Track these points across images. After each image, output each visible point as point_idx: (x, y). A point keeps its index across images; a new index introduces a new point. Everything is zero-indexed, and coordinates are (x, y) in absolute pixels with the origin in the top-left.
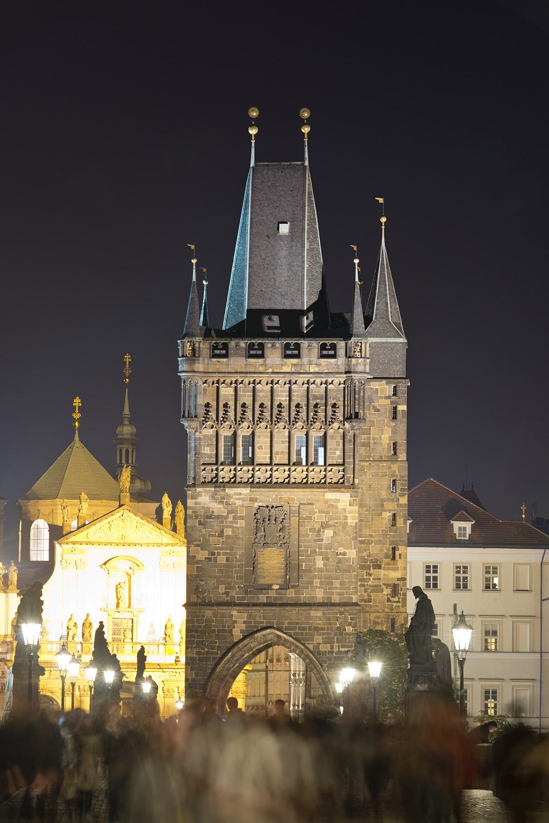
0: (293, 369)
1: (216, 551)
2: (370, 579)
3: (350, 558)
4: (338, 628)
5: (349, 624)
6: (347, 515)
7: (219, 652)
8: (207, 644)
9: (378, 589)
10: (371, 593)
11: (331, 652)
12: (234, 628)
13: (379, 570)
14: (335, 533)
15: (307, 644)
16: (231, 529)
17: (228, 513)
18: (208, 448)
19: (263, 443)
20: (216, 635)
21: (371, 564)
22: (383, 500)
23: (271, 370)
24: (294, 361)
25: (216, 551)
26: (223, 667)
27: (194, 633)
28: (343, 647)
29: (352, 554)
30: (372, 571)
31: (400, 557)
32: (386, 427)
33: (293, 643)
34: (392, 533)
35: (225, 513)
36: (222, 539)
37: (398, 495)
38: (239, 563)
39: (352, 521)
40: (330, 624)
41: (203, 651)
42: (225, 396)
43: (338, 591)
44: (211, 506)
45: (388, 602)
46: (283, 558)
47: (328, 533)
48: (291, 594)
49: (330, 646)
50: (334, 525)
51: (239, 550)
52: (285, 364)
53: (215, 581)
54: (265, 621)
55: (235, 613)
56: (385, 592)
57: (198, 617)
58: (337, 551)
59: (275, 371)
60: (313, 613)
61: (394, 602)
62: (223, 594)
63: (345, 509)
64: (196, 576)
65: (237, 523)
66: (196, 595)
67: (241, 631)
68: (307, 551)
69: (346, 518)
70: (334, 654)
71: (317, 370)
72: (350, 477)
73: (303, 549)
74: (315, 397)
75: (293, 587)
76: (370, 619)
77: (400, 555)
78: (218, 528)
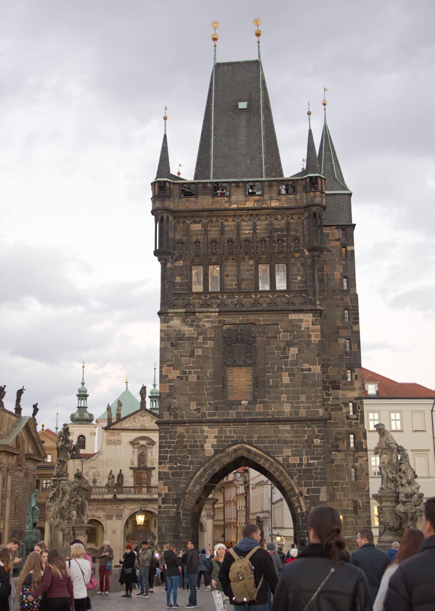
0: (255, 204)
1: (187, 371)
2: (329, 399)
4: (305, 440)
5: (317, 437)
6: (310, 333)
7: (192, 466)
8: (179, 459)
10: (331, 411)
11: (301, 464)
13: (338, 391)
14: (299, 350)
15: (277, 457)
17: (198, 335)
18: (179, 278)
19: (230, 272)
20: (188, 450)
21: (330, 385)
22: (339, 328)
23: (234, 206)
24: (257, 198)
25: (187, 371)
26: (196, 482)
27: (167, 449)
28: (312, 459)
29: (317, 369)
30: (331, 391)
31: (356, 379)
32: (337, 265)
33: (263, 457)
34: (348, 357)
35: (195, 335)
37: (351, 323)
38: (209, 381)
39: (315, 339)
40: (298, 437)
41: (175, 466)
42: (194, 231)
43: (305, 405)
44: (182, 329)
45: (347, 419)
46: (251, 375)
47: (294, 351)
50: (298, 344)
51: (209, 369)
52: (248, 201)
53: (186, 398)
54: (235, 435)
55: (206, 428)
56: (344, 411)
57: (171, 433)
58: (302, 367)
59: (240, 206)
60: (281, 427)
61: (353, 419)
62: (194, 410)
63: (308, 328)
64: (169, 395)
65: (206, 344)
66: (168, 413)
67: (213, 446)
68: (274, 368)
69: (310, 336)
70: (304, 466)
72: (312, 299)
73: (269, 366)
74: (276, 230)
75: (260, 403)
76: (332, 436)
78: (188, 349)
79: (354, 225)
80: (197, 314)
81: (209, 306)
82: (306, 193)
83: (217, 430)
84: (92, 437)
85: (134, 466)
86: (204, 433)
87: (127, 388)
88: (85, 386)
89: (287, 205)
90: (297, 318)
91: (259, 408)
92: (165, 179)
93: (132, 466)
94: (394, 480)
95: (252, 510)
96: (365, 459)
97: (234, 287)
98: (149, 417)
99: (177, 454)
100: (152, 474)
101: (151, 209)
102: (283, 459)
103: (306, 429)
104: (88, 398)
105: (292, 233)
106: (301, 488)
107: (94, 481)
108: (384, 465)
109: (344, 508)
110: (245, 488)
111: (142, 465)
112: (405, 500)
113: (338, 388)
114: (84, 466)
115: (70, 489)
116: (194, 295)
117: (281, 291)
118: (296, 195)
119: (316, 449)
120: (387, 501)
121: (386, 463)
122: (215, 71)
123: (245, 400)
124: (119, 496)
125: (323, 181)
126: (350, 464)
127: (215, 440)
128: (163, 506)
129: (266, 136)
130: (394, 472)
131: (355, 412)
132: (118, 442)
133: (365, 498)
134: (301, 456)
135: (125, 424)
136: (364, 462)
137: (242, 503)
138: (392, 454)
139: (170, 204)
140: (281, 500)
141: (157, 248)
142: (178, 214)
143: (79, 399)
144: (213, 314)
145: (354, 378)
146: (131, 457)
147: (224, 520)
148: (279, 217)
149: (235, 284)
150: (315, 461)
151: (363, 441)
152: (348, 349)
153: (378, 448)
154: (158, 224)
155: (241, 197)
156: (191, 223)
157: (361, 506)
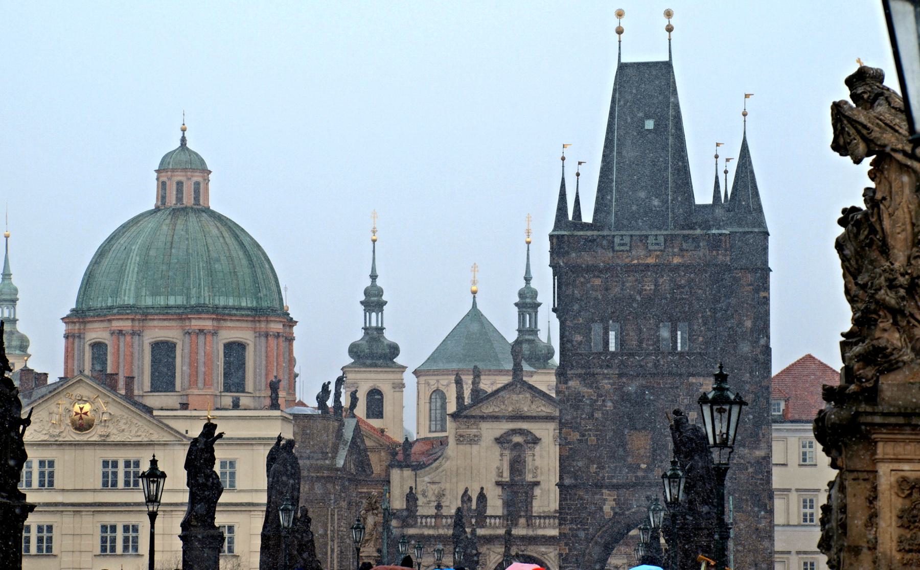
23: (636, 262)
55: (605, 491)
64: (568, 457)
84: (398, 394)
87: (474, 304)
88: (379, 283)
92: (565, 233)
93: (500, 479)
98: (528, 395)
100: (535, 494)
104: (385, 307)
107: (439, 507)
124: (480, 532)
135: (488, 409)
142: (576, 269)
146: (498, 464)
155: (642, 253)
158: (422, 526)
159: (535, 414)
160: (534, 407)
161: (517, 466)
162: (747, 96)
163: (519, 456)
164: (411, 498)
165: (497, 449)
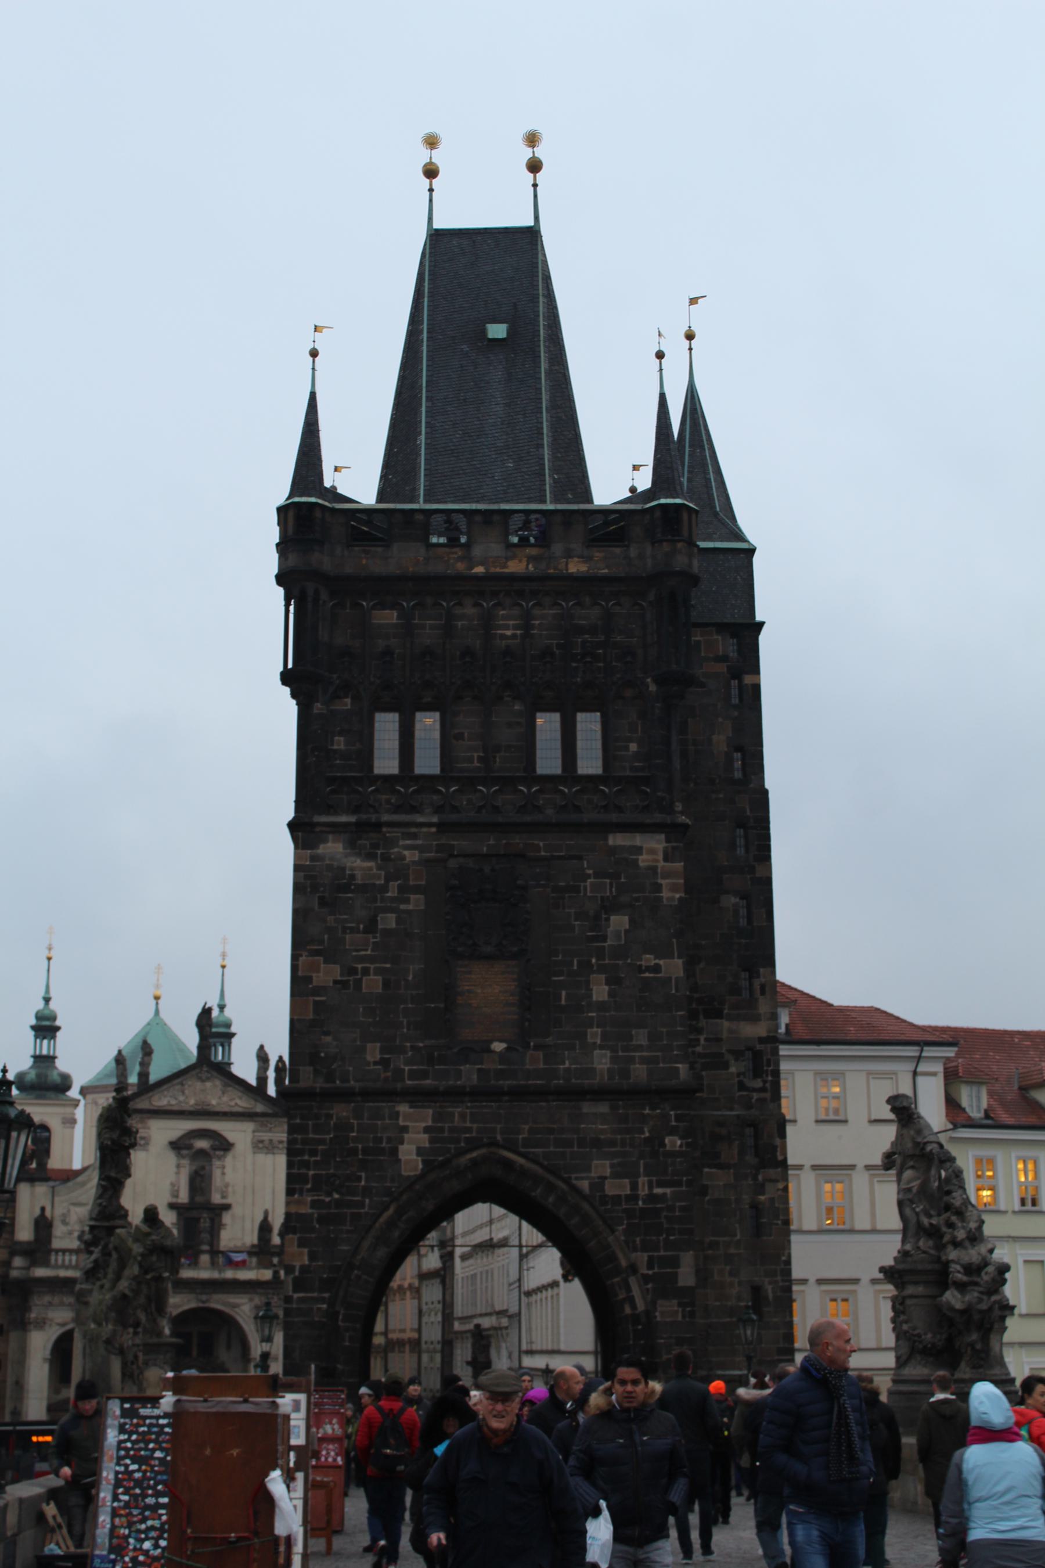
0: (530, 566)
1: (359, 966)
2: (698, 1040)
3: (670, 978)
5: (673, 1131)
6: (659, 881)
7: (367, 1201)
8: (337, 1182)
9: (717, 1062)
11: (633, 1198)
12: (402, 1143)
14: (632, 921)
16: (394, 915)
18: (342, 739)
23: (480, 570)
25: (359, 966)
27: (306, 1157)
28: (660, 1184)
29: (674, 967)
30: (703, 1022)
31: (763, 992)
32: (720, 720)
34: (743, 941)
35: (379, 878)
36: (375, 937)
38: (414, 992)
39: (670, 895)
41: (327, 1199)
47: (619, 922)
48: (534, 1061)
49: (631, 1183)
52: (513, 557)
54: (475, 1126)
55: (403, 1108)
56: (733, 1069)
59: (492, 570)
60: (587, 1108)
62: (375, 1063)
63: (653, 869)
65: (407, 901)
66: (311, 1068)
67: (420, 1151)
69: (658, 888)
70: (640, 1203)
71: (584, 568)
75: (537, 1047)
77: (763, 988)
79: (761, 624)
80: (384, 829)
81: (414, 809)
82: (653, 544)
83: (430, 1111)
85: (180, 1201)
86: (397, 1119)
88: (53, 1005)
89: (606, 571)
90: (628, 843)
91: (534, 1061)
92: (313, 500)
93: (174, 1200)
94: (933, 1233)
95: (459, 1311)
96: (781, 1186)
97: (476, 764)
98: (218, 1083)
99: (332, 1171)
101: (276, 571)
102: (591, 1185)
103: (647, 1111)
104: (58, 1034)
105: (619, 639)
106: (633, 1255)
108: (909, 1196)
109: (729, 1303)
110: (442, 1257)
111: (199, 1199)
112: (965, 1278)
113: (719, 1015)
114: (56, 1199)
115: (141, 1250)
116: (379, 783)
117: (590, 778)
118: (628, 546)
119: (669, 1160)
120: (916, 1283)
121: (915, 1190)
122: (430, 248)
123: (501, 1041)
125: (694, 516)
126: (746, 1198)
127: (426, 1136)
128: (296, 1296)
129: (553, 406)
130: (932, 1212)
131: (757, 1071)
132: (142, 1142)
133: (779, 1278)
134: (633, 1176)
135: (162, 1100)
136: (780, 1193)
137: (432, 1293)
138: (929, 1169)
139: (325, 561)
140: (554, 1284)
141: (290, 666)
143: (36, 1037)
144: (425, 830)
145: (759, 992)
147: (385, 1334)
148: (587, 600)
149: (479, 757)
150: (668, 1191)
151: (778, 1141)
152: (743, 922)
153: (894, 1153)
154: (292, 608)
155: (496, 549)
156: (374, 608)
157: (771, 1296)
158: (57, 1267)
159: (226, 1109)
160: (225, 1099)
161: (199, 1182)
162: (693, 301)
163: (203, 1168)
164: (43, 1225)
165: (171, 1158)
